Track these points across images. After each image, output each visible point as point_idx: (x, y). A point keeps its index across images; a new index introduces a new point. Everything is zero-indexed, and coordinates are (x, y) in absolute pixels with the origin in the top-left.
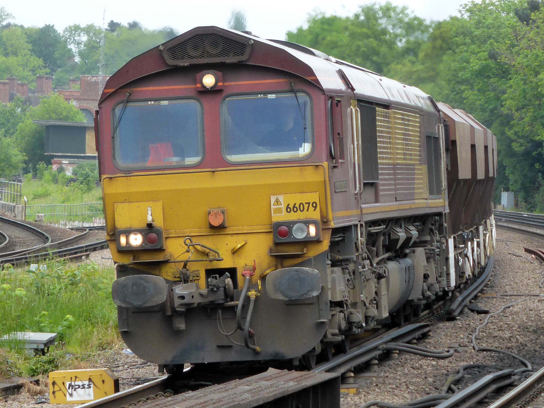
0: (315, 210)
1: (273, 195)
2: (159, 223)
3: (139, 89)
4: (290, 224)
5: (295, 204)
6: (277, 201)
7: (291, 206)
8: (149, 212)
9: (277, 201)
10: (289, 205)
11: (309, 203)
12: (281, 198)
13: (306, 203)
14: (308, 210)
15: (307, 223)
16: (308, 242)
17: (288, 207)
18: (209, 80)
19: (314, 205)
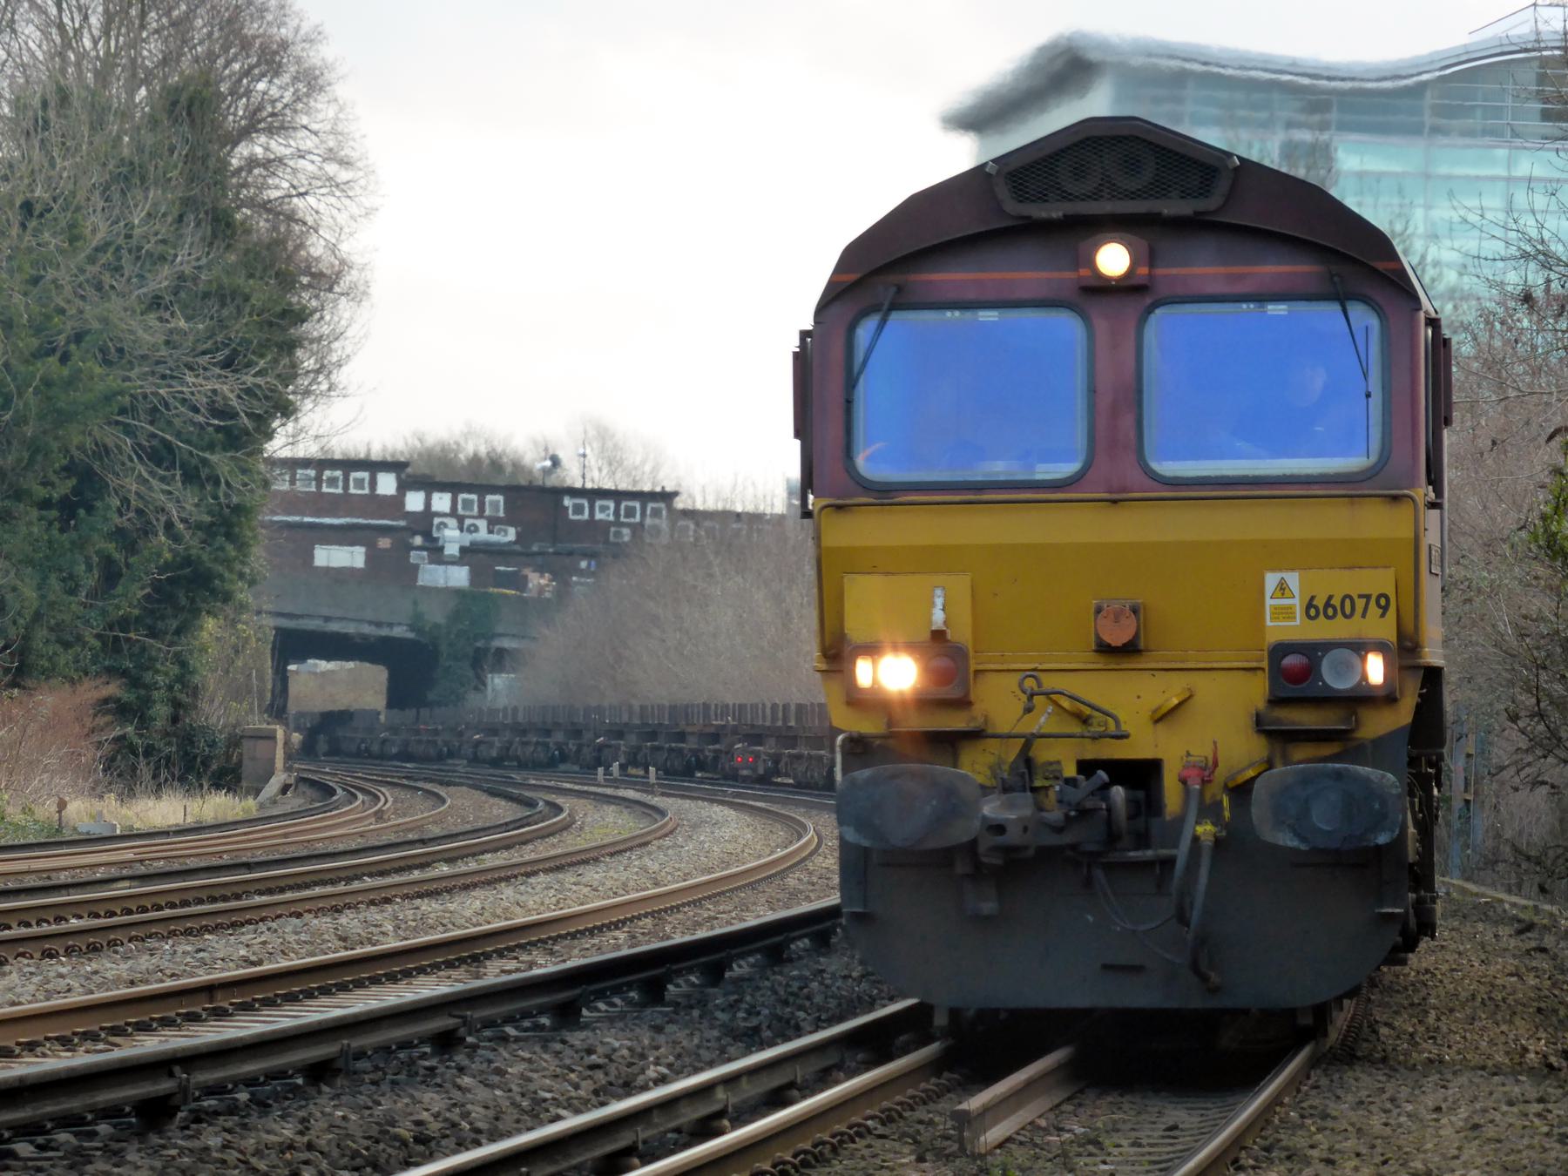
0: (1383, 615)
1: (1273, 569)
4: (1314, 651)
5: (1330, 597)
6: (1282, 588)
8: (939, 602)
9: (1282, 588)
10: (1313, 598)
11: (1368, 597)
12: (1293, 579)
14: (1364, 616)
16: (1363, 698)
18: (1113, 259)
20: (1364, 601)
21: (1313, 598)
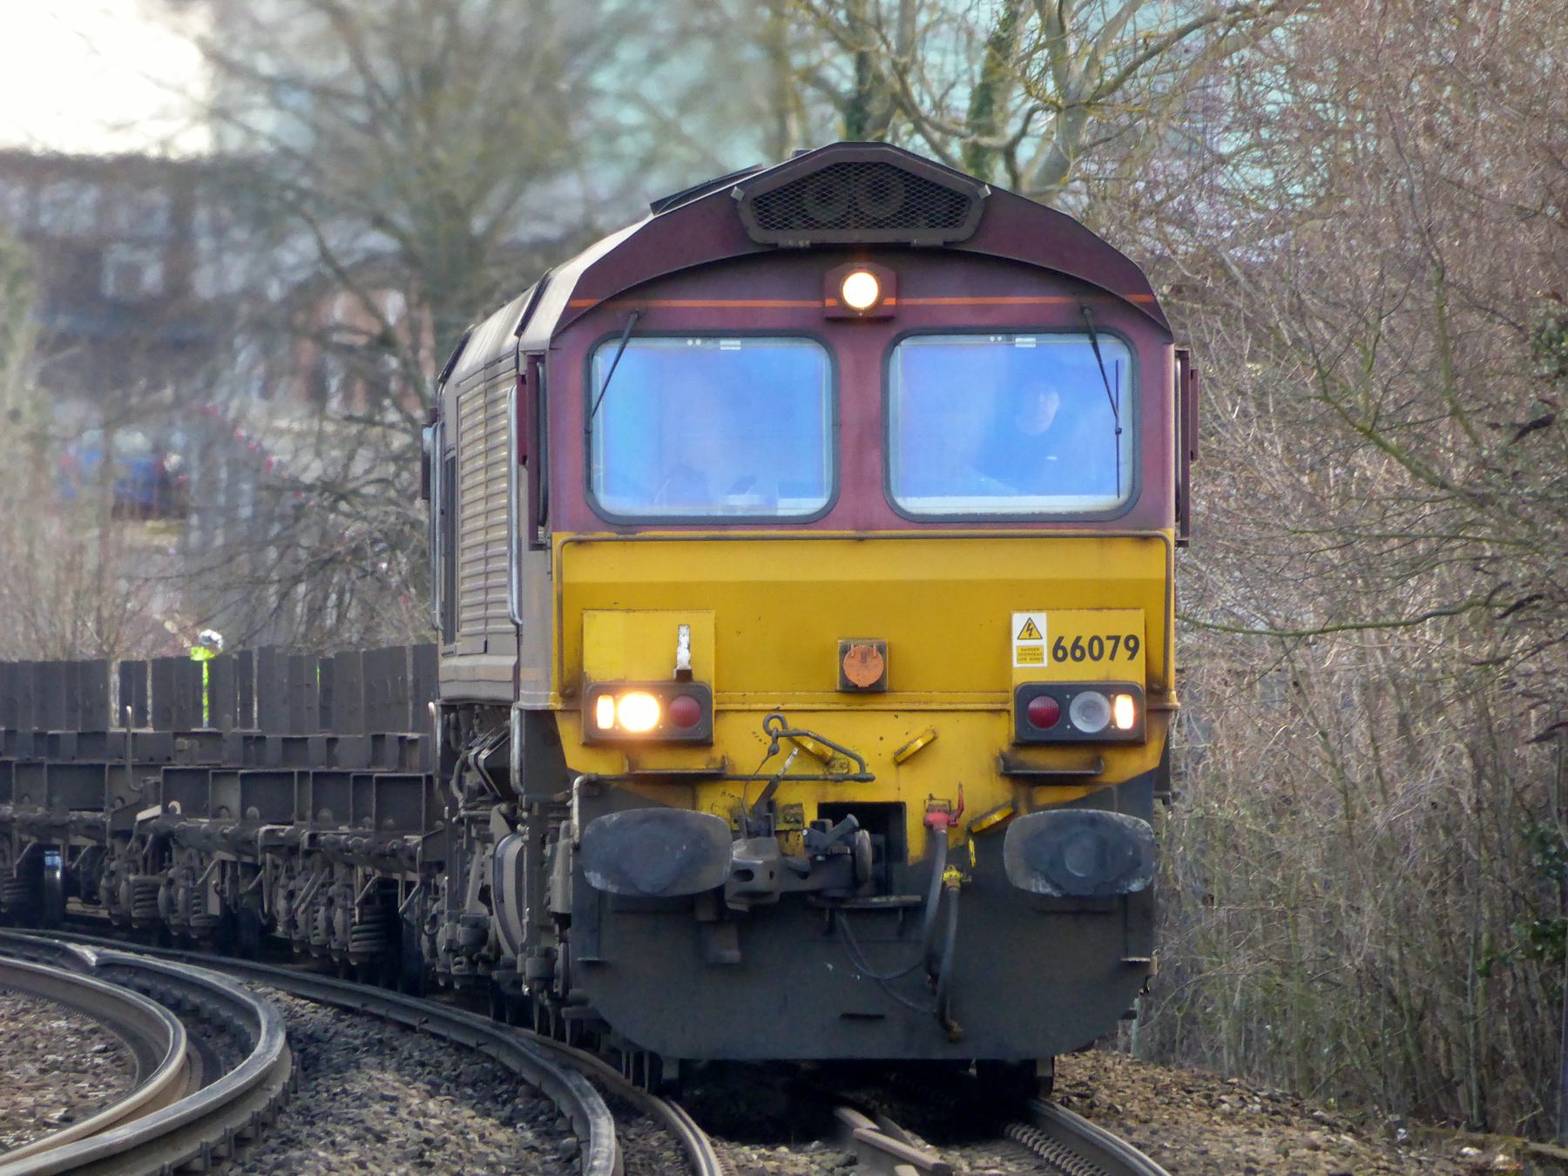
0: (1131, 657)
1: (1020, 610)
2: (705, 673)
3: (666, 303)
4: (1063, 693)
5: (1078, 639)
6: (1030, 628)
7: (1068, 644)
8: (684, 640)
9: (1030, 628)
10: (1060, 639)
11: (1117, 639)
12: (1040, 620)
13: (1109, 638)
14: (1112, 657)
15: (1110, 690)
17: (1058, 646)
18: (861, 290)
19: (1132, 644)
20: (1112, 642)
21: (1060, 639)
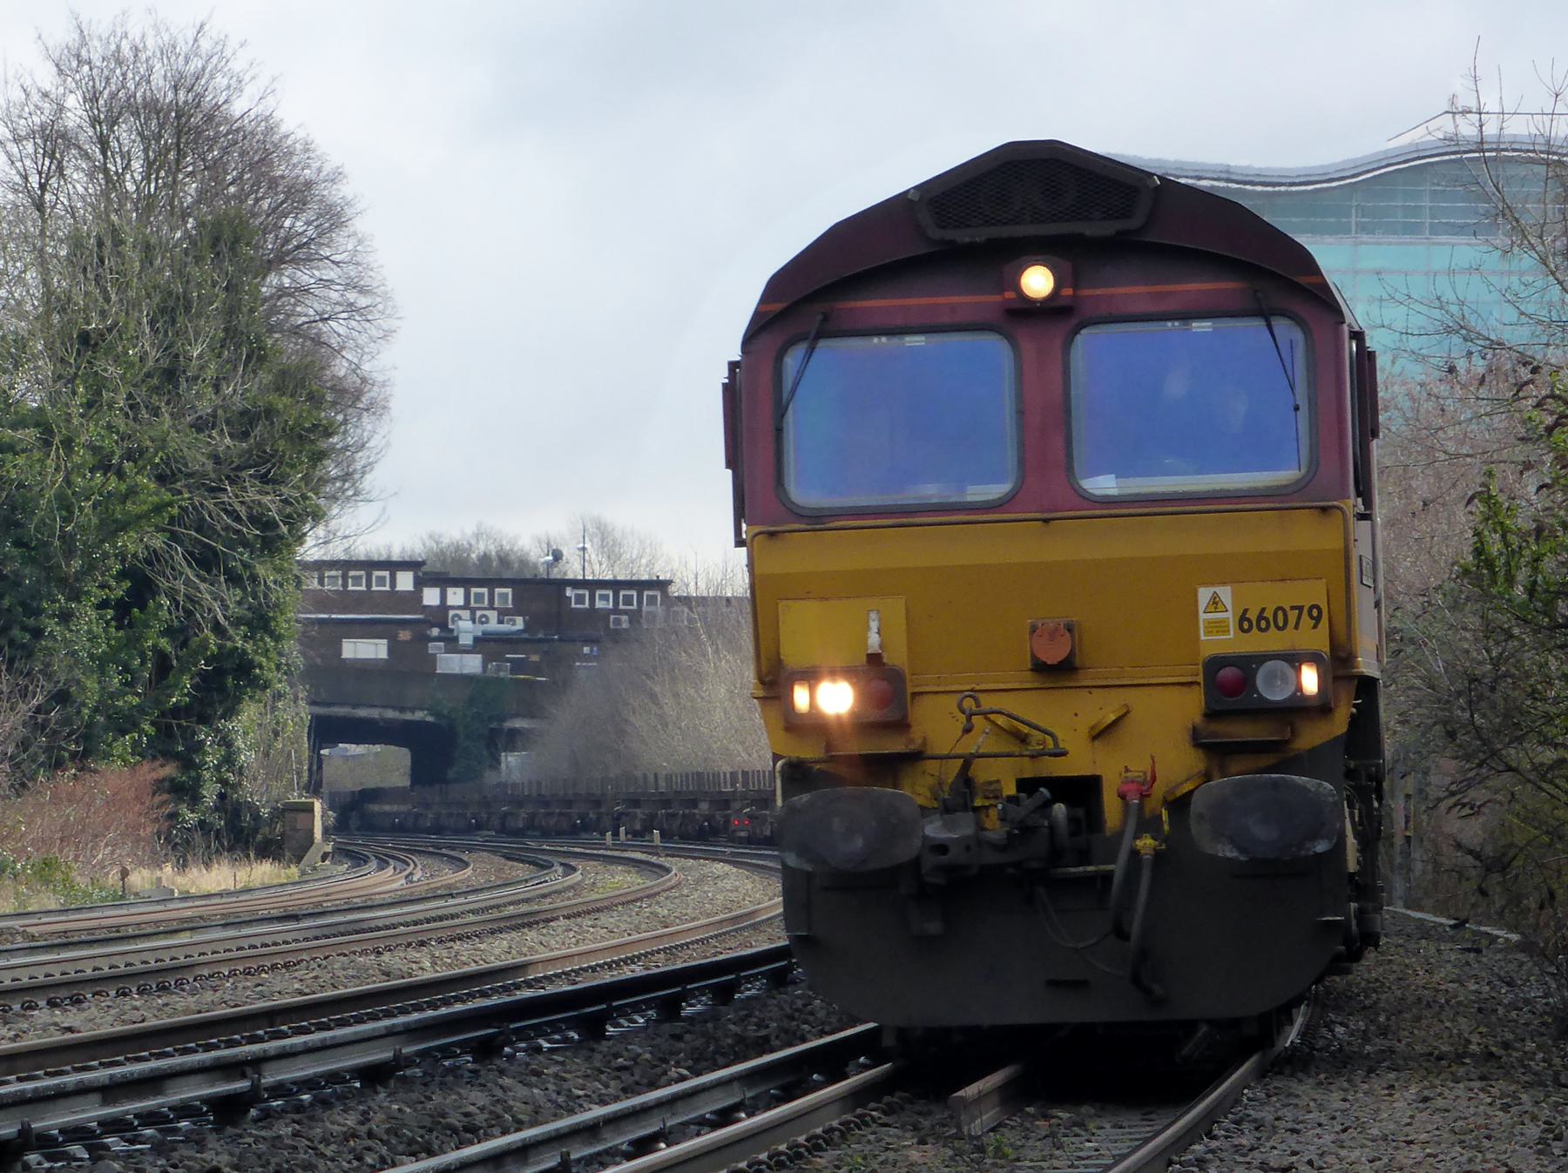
0: (1315, 627)
1: (1205, 584)
3: (852, 304)
4: (1248, 664)
5: (1263, 610)
6: (1215, 602)
7: (1253, 616)
8: (874, 625)
9: (1215, 602)
10: (1246, 611)
11: (1300, 608)
12: (1225, 593)
13: (1293, 608)
14: (1297, 627)
15: (1295, 660)
17: (1243, 618)
18: (1037, 281)
21: (1246, 611)
